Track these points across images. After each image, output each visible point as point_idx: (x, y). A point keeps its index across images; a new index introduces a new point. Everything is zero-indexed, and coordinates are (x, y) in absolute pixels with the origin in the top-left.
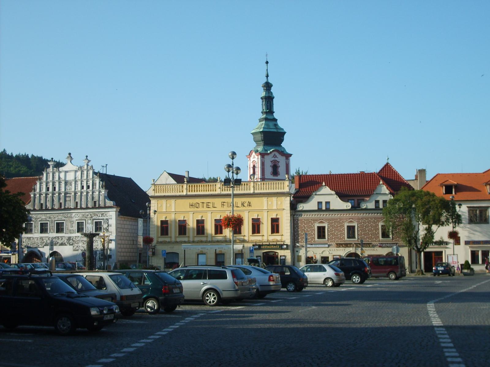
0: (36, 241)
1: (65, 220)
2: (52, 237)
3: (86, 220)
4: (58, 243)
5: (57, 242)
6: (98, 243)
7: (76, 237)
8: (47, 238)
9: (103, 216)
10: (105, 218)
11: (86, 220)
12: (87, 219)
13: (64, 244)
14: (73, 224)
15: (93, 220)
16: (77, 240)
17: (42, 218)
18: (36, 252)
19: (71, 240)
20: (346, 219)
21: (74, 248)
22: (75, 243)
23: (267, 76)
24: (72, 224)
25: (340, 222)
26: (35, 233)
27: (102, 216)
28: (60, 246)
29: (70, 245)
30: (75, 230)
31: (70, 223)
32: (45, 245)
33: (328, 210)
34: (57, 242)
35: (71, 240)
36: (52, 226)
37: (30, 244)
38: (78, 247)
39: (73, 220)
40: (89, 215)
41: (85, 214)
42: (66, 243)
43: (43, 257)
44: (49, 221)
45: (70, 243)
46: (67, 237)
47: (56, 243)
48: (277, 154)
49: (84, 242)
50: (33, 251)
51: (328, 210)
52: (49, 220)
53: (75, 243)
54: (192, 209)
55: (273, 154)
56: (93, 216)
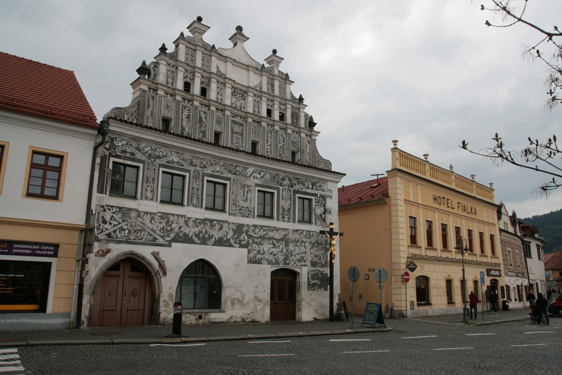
0: (149, 224)
1: (228, 179)
2: (197, 219)
3: (279, 188)
4: (211, 237)
5: (209, 235)
6: (305, 247)
7: (255, 226)
8: (181, 221)
9: (314, 188)
10: (319, 193)
11: (279, 188)
12: (281, 188)
13: (226, 242)
14: (249, 194)
15: (296, 192)
16: (258, 235)
17: (170, 158)
18: (143, 258)
19: (243, 233)
21: (251, 255)
22: (254, 242)
24: (246, 194)
26: (147, 198)
27: (312, 189)
28: (212, 246)
29: (241, 246)
30: (254, 208)
31: (242, 191)
32: (175, 240)
34: (209, 235)
35: (244, 235)
37: (127, 232)
38: (262, 252)
39: (248, 182)
40: (287, 179)
41: (277, 175)
42: (232, 241)
43: (165, 274)
44: (189, 171)
45: (242, 241)
46: (233, 223)
47: (207, 236)
49: (275, 242)
50: (136, 255)
52: (189, 169)
53: (253, 240)
56: (295, 184)
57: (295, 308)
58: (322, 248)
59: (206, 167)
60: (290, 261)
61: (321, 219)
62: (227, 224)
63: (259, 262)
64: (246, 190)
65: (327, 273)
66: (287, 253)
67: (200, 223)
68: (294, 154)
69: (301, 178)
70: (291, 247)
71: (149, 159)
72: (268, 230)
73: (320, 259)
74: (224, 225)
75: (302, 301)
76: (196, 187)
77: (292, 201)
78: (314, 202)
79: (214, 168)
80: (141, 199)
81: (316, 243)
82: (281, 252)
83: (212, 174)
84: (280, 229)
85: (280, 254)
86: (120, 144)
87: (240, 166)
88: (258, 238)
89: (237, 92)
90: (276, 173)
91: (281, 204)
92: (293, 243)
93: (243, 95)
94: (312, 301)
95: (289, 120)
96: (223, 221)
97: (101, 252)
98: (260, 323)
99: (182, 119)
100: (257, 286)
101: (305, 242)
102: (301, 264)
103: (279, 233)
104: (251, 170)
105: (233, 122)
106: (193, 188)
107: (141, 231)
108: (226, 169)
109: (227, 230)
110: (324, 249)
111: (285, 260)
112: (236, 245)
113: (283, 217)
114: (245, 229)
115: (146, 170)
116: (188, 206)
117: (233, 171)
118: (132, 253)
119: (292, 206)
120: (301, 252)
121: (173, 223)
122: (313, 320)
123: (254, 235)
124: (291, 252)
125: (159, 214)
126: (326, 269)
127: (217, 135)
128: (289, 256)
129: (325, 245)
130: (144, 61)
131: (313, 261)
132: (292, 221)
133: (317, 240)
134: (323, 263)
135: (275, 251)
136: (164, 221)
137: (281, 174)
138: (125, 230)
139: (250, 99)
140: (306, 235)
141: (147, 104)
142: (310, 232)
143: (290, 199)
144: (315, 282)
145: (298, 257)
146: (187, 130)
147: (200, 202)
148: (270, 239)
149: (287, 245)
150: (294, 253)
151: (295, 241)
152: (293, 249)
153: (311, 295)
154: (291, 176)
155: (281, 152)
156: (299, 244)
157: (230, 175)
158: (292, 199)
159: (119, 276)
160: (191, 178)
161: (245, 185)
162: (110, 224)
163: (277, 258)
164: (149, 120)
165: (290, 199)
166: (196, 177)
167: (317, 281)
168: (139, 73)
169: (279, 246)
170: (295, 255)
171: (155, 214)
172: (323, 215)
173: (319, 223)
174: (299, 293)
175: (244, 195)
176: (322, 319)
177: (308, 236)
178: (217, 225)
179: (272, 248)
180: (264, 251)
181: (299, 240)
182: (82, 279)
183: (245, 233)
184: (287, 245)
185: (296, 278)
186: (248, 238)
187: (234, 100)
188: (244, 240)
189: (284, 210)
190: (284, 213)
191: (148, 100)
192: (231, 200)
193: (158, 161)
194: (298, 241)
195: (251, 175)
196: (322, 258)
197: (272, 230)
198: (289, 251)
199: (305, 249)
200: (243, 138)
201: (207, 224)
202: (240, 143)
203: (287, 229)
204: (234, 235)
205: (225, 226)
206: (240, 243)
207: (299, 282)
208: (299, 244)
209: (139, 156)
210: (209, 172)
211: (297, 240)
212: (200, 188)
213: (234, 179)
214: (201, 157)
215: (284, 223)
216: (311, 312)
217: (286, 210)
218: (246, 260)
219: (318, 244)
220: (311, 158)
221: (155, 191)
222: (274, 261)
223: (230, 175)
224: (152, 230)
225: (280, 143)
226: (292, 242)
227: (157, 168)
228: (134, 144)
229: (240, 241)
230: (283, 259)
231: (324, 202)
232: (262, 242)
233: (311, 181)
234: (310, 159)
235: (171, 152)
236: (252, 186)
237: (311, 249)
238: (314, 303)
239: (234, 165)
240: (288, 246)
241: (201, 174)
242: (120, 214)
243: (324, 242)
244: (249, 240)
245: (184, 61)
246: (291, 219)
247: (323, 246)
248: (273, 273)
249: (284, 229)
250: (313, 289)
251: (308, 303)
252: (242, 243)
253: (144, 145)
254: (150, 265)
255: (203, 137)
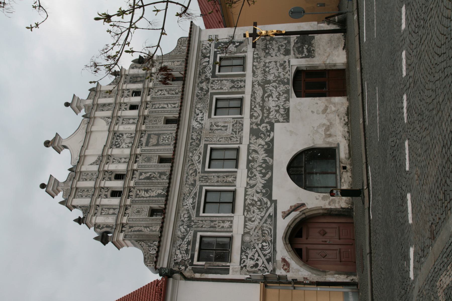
0: (256, 223)
1: (206, 146)
3: (211, 93)
5: (263, 163)
6: (270, 62)
7: (251, 116)
8: (250, 191)
9: (208, 55)
10: (213, 50)
12: (211, 91)
13: (269, 146)
14: (220, 124)
15: (214, 75)
16: (260, 113)
18: (289, 226)
19: (259, 128)
21: (281, 119)
22: (268, 117)
24: (219, 128)
26: (231, 227)
27: (209, 57)
28: (274, 159)
29: (272, 129)
30: (233, 118)
31: (217, 132)
32: (270, 196)
34: (263, 163)
35: (261, 127)
37: (264, 244)
38: (277, 108)
39: (207, 126)
40: (201, 85)
41: (197, 96)
42: (268, 139)
43: (303, 205)
44: (201, 187)
45: (267, 129)
46: (250, 139)
47: (264, 165)
49: (266, 95)
50: (286, 233)
52: (198, 187)
53: (266, 118)
56: (206, 76)
57: (333, 70)
58: (270, 44)
59: (196, 169)
60: (285, 78)
61: (240, 47)
62: (251, 145)
63: (287, 111)
64: (215, 127)
65: (296, 38)
66: (277, 82)
67: (252, 173)
69: (198, 69)
70: (270, 77)
71: (192, 227)
72: (255, 102)
73: (282, 46)
74: (252, 148)
75: (325, 63)
76: (216, 179)
77: (224, 78)
78: (223, 55)
79: (195, 162)
80: (232, 232)
81: (265, 51)
82: (276, 88)
83: (203, 163)
84: (252, 90)
85: (278, 89)
86: (180, 256)
87: (192, 135)
88: (263, 113)
89: (116, 142)
90: (195, 98)
91: (227, 91)
92: (266, 75)
93: (118, 136)
94: (326, 53)
96: (248, 149)
97: (285, 267)
98: (349, 107)
99: (150, 197)
100: (312, 111)
101: (265, 63)
102: (287, 66)
103: (257, 90)
104: (194, 124)
105: (147, 145)
106: (218, 182)
107: (263, 230)
108: (196, 150)
109: (257, 145)
110: (271, 42)
111: (284, 83)
112: (272, 135)
113: (241, 87)
114: (255, 127)
115: (203, 229)
116: (235, 186)
117: (197, 142)
118: (285, 238)
119: (228, 79)
120: (275, 66)
121: (253, 200)
122: (345, 51)
123: (260, 117)
124: (276, 77)
125: (246, 213)
126: (291, 39)
127: (162, 160)
128: (280, 79)
129: (267, 41)
130: (94, 239)
131: (284, 53)
132: (244, 78)
133: (263, 49)
134: (286, 42)
135: (275, 94)
136: (252, 209)
137: (196, 92)
138: (263, 246)
139: (121, 128)
140: (257, 62)
141: (138, 233)
142: (254, 58)
143: (221, 80)
144: (305, 50)
145: (280, 70)
146: (160, 191)
147: (230, 174)
148: (263, 100)
149: (269, 82)
150: (277, 74)
151: (264, 73)
152: (273, 75)
153: (319, 54)
154: (198, 81)
155: (174, 92)
156: (267, 69)
157: (202, 145)
158: (221, 79)
159: (307, 248)
160: (208, 184)
161: (211, 129)
162: (257, 260)
163: (283, 92)
164: (154, 229)
165: (221, 80)
166: (207, 179)
167: (305, 48)
168: (107, 243)
169: (271, 90)
170: (279, 73)
171: (245, 217)
172: (235, 44)
173: (244, 49)
174: (318, 67)
175: (221, 129)
176: (344, 41)
177: (259, 60)
178: (252, 156)
179: (272, 97)
180: (276, 106)
181: (263, 69)
182: (312, 283)
183: (259, 127)
184: (269, 82)
185: (302, 70)
186: (264, 123)
187: (124, 145)
188: (266, 127)
189: (233, 87)
190: (236, 86)
191: (134, 231)
192: (227, 143)
193: (194, 218)
194: (264, 70)
195: (200, 124)
196: (280, 44)
197: (255, 98)
198: (275, 79)
199: (272, 63)
200: (163, 134)
201: (252, 166)
202: (168, 136)
203: (253, 82)
204: (261, 138)
205: (253, 147)
206: (270, 132)
207: (306, 67)
208: (267, 69)
209: (190, 237)
210: (200, 166)
211: (263, 72)
212: (217, 174)
213: (205, 141)
214: (186, 175)
215: (246, 86)
216: (337, 53)
217: (233, 84)
218: (286, 124)
219: (266, 48)
220: (177, 60)
221: (224, 219)
222: (286, 95)
223: (202, 145)
224: (261, 220)
225: (164, 95)
226: (265, 76)
227: (201, 219)
228: (179, 243)
229: (267, 131)
230: (284, 86)
231: (223, 44)
232: (267, 108)
233: (201, 60)
234: (178, 61)
235: (183, 206)
236: (211, 121)
237: (272, 56)
238: (328, 50)
239: (191, 141)
240: (270, 81)
241: (203, 175)
242: (248, 251)
243: (263, 42)
244: (265, 121)
245: (90, 199)
246: (242, 79)
247: (268, 43)
248: (298, 95)
249: (253, 86)
250: (313, 52)
251: (328, 57)
252: (269, 129)
253: (179, 233)
254: (295, 219)
255: (165, 175)
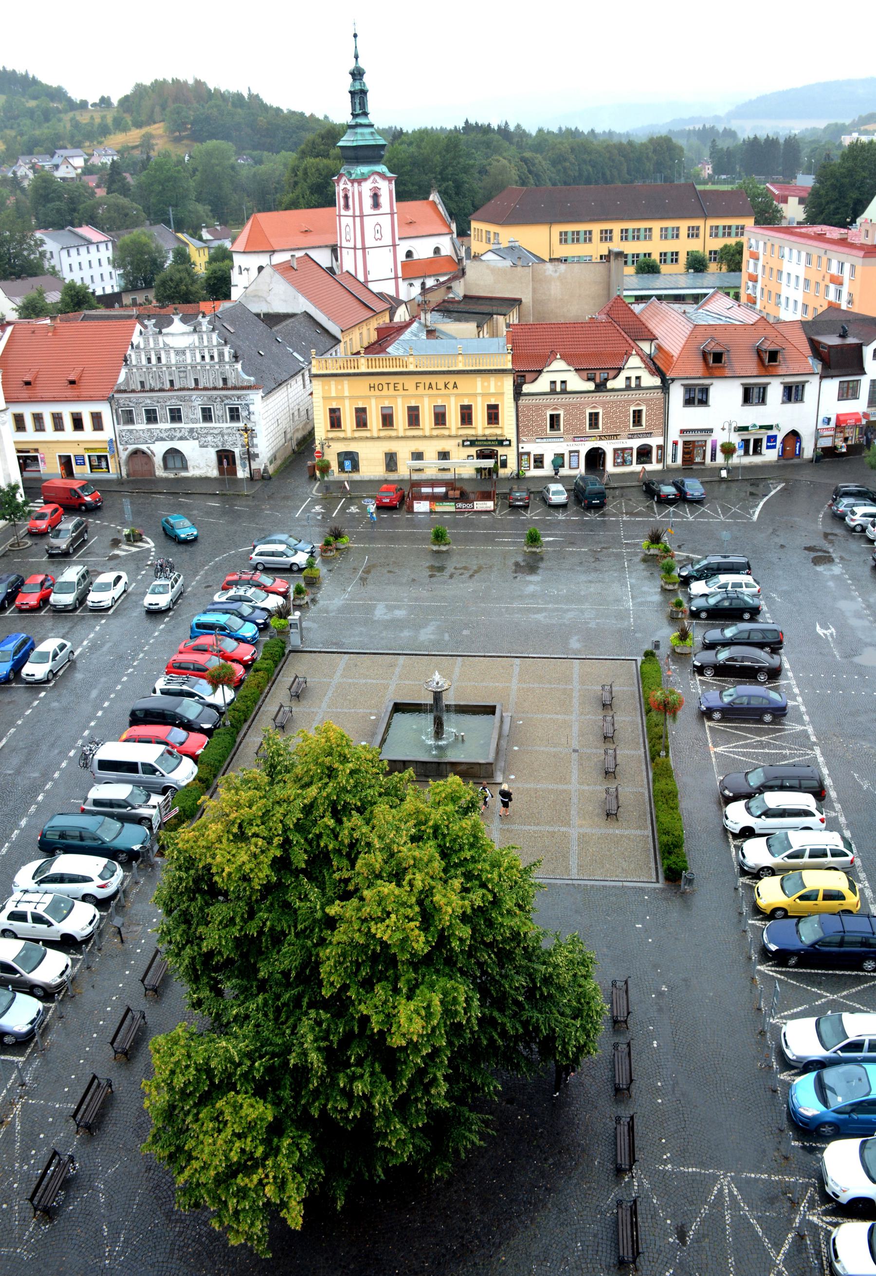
10: (243, 403)
20: (588, 404)
23: (356, 57)
25: (580, 408)
33: (564, 391)
36: (163, 413)
48: (377, 178)
51: (564, 391)
54: (372, 393)
55: (372, 178)
68: (225, 380)
70: (226, 437)
95: (216, 359)
127: (172, 382)
